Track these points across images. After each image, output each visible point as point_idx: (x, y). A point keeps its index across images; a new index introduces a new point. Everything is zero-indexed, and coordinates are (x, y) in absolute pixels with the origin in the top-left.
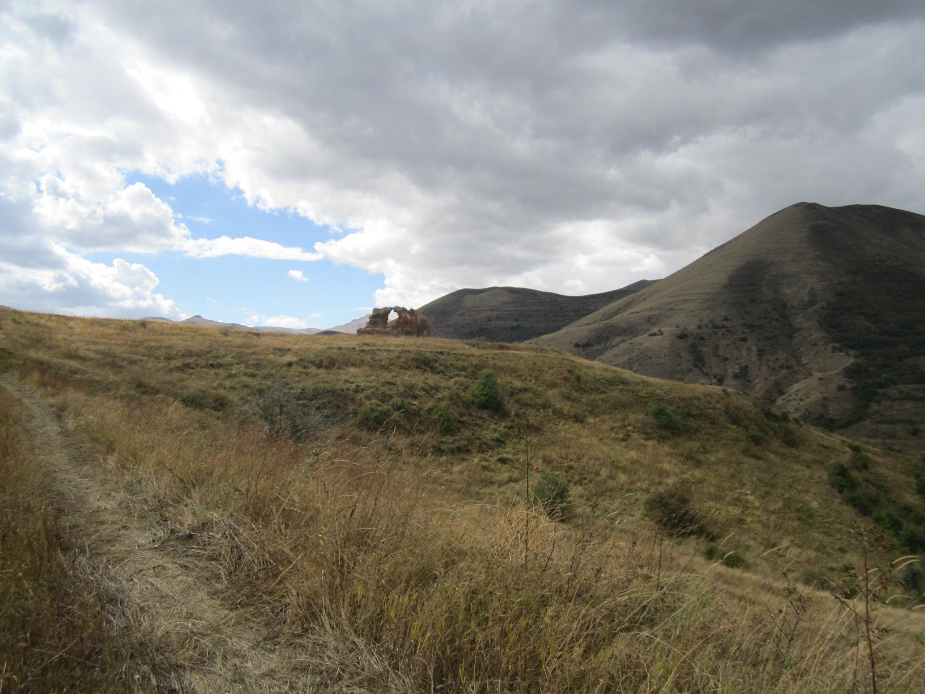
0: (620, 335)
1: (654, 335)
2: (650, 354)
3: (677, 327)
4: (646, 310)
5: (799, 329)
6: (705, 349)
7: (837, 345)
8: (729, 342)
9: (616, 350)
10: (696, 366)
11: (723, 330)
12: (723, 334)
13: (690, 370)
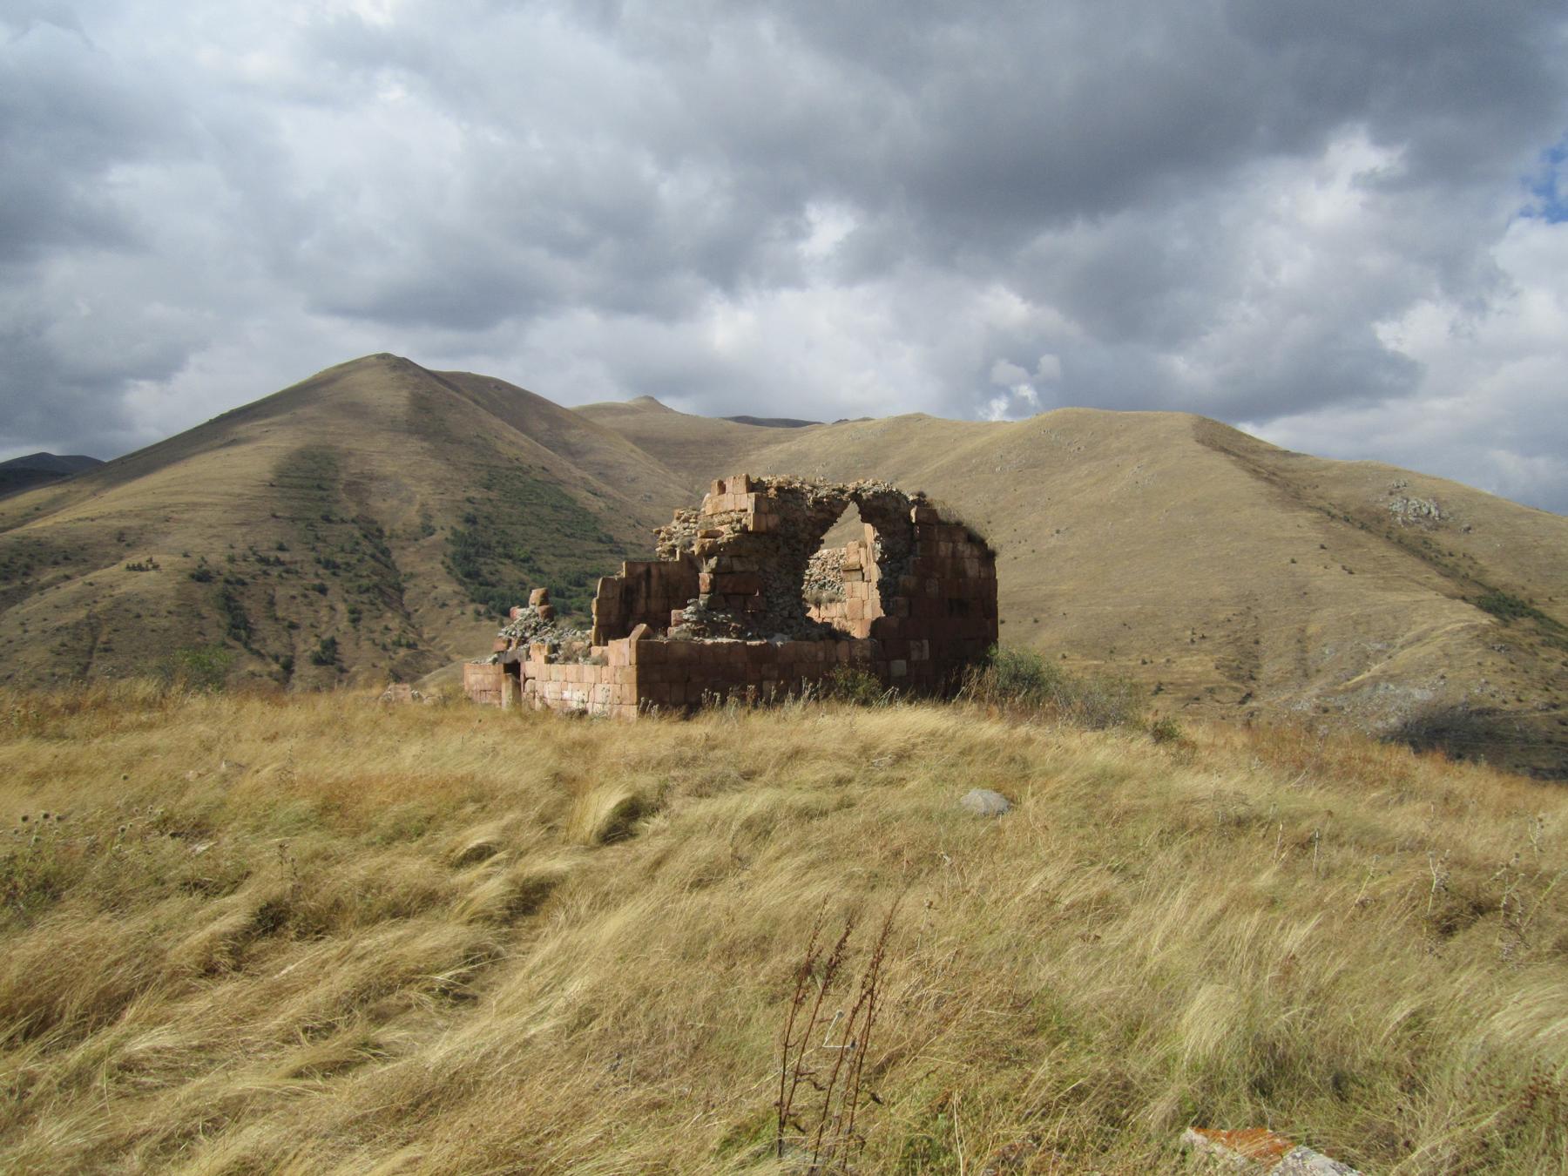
0: (56, 563)
1: (139, 568)
2: (136, 609)
3: (186, 555)
4: (109, 516)
6: (247, 603)
7: (482, 609)
8: (293, 593)
9: (52, 596)
10: (238, 639)
11: (281, 568)
12: (280, 576)
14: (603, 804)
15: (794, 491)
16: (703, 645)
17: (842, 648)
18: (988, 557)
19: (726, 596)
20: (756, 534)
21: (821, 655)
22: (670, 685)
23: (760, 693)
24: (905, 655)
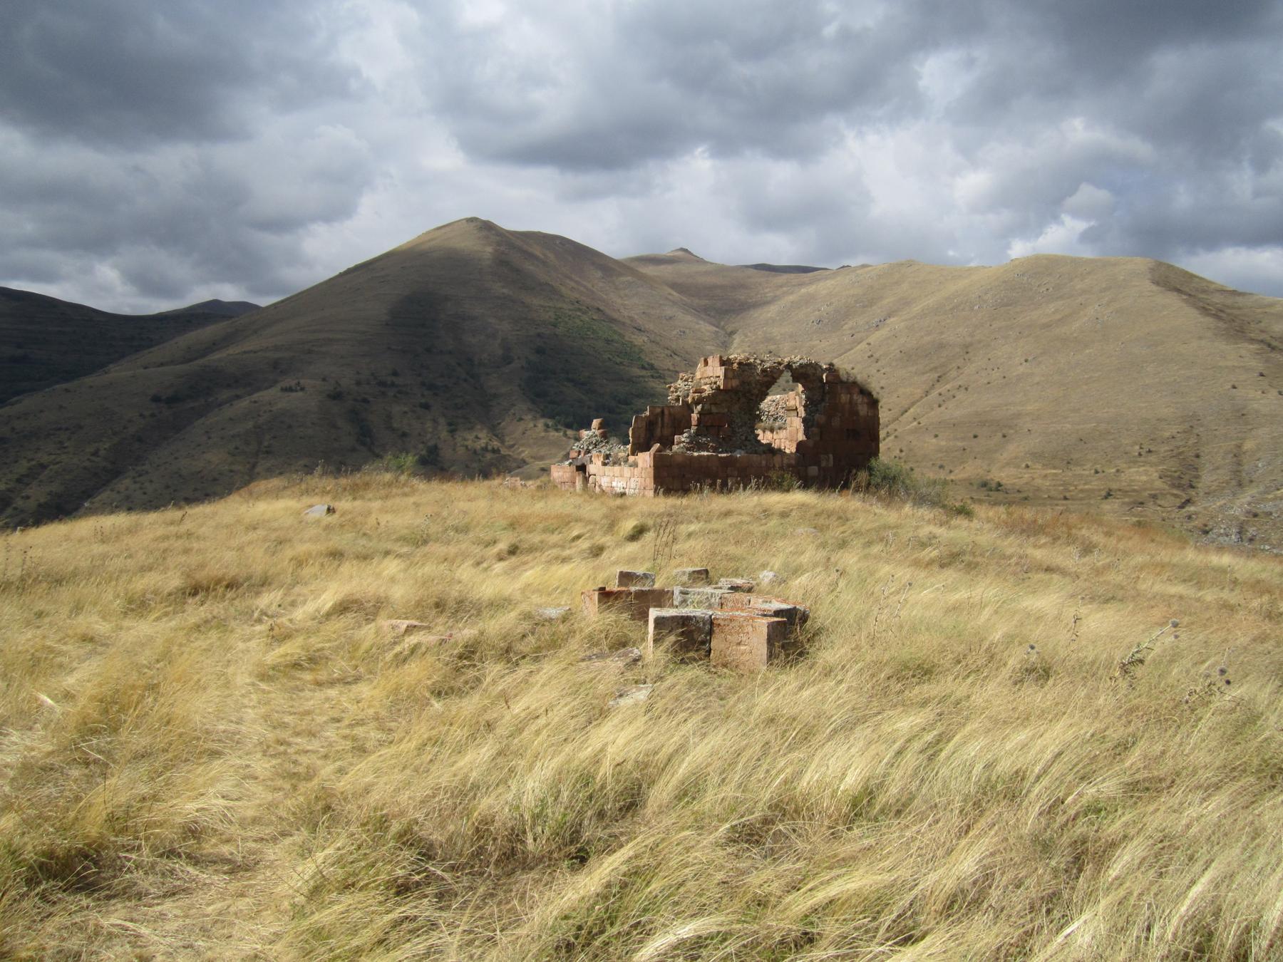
0: (229, 386)
1: (290, 389)
3: (324, 380)
5: (495, 396)
7: (550, 423)
10: (364, 444)
13: (354, 450)
14: (628, 525)
15: (750, 364)
16: (692, 457)
17: (777, 459)
18: (874, 403)
19: (707, 427)
20: (725, 391)
21: (764, 463)
22: (671, 478)
23: (724, 484)
24: (817, 463)
